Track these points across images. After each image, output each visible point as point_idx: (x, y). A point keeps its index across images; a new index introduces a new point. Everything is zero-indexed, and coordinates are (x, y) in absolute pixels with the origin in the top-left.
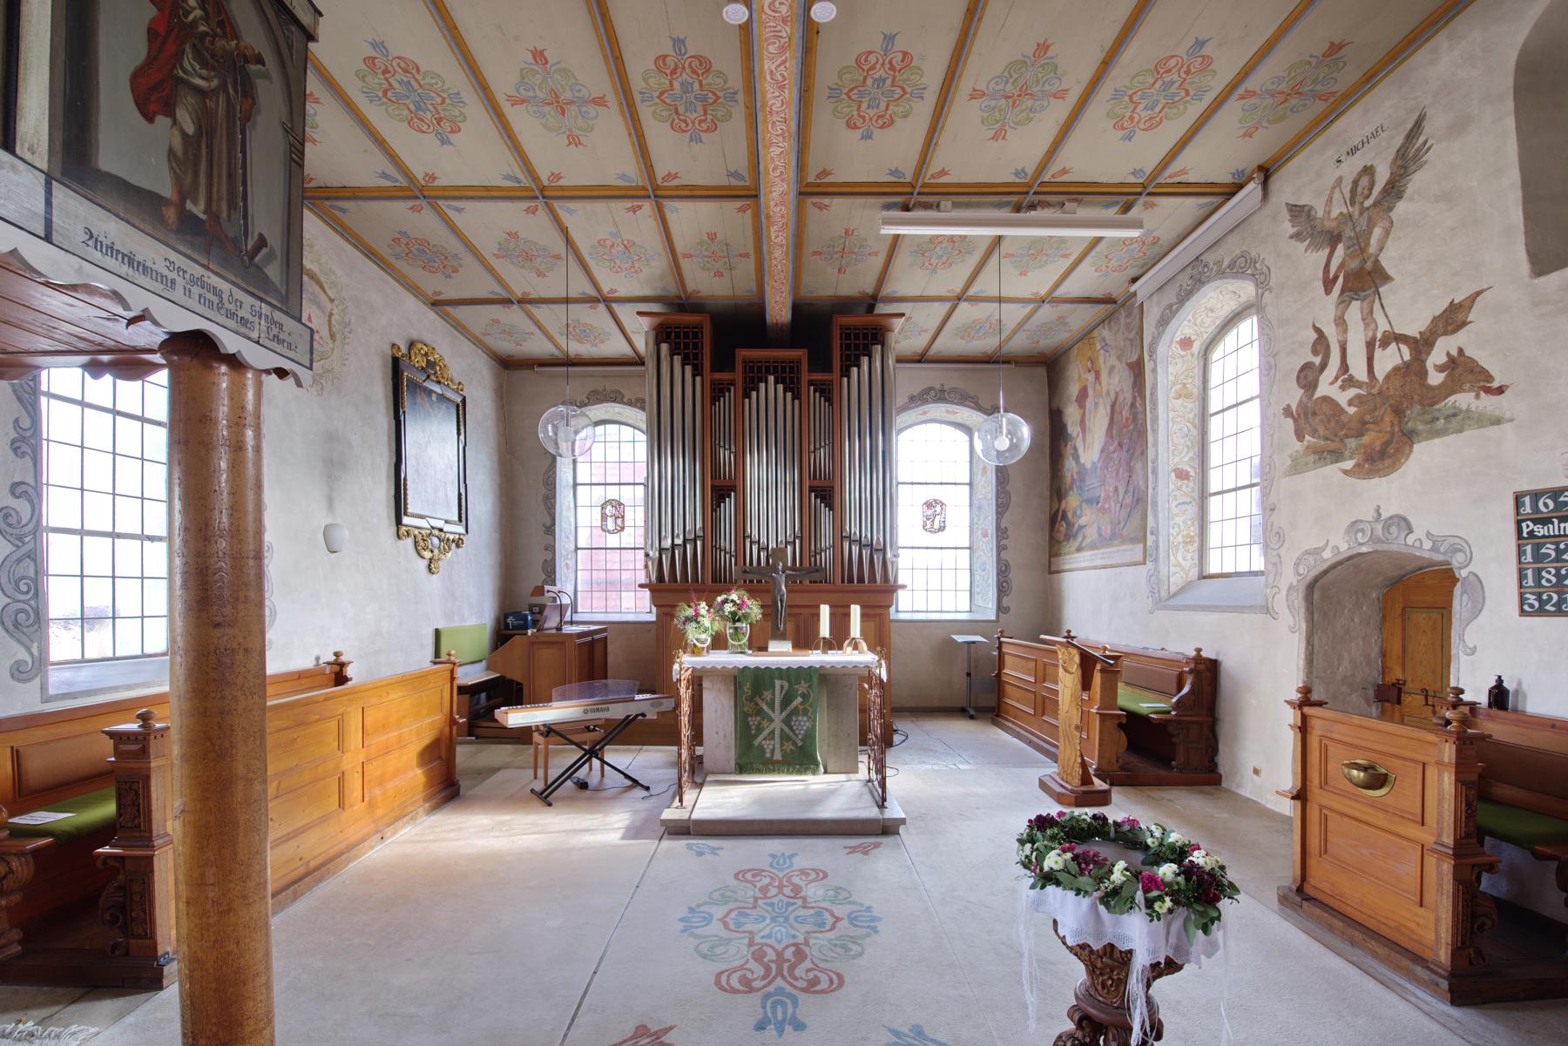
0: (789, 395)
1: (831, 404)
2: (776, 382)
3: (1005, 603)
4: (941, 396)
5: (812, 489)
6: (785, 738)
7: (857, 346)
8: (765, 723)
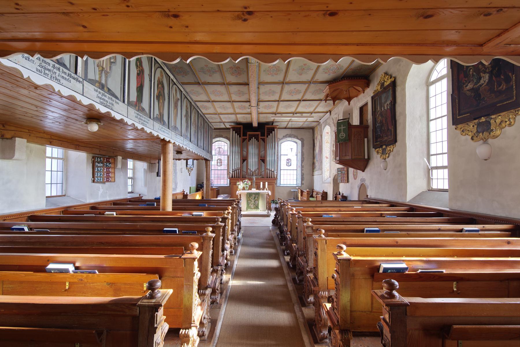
3: (303, 182)
4: (290, 136)
6: (254, 204)
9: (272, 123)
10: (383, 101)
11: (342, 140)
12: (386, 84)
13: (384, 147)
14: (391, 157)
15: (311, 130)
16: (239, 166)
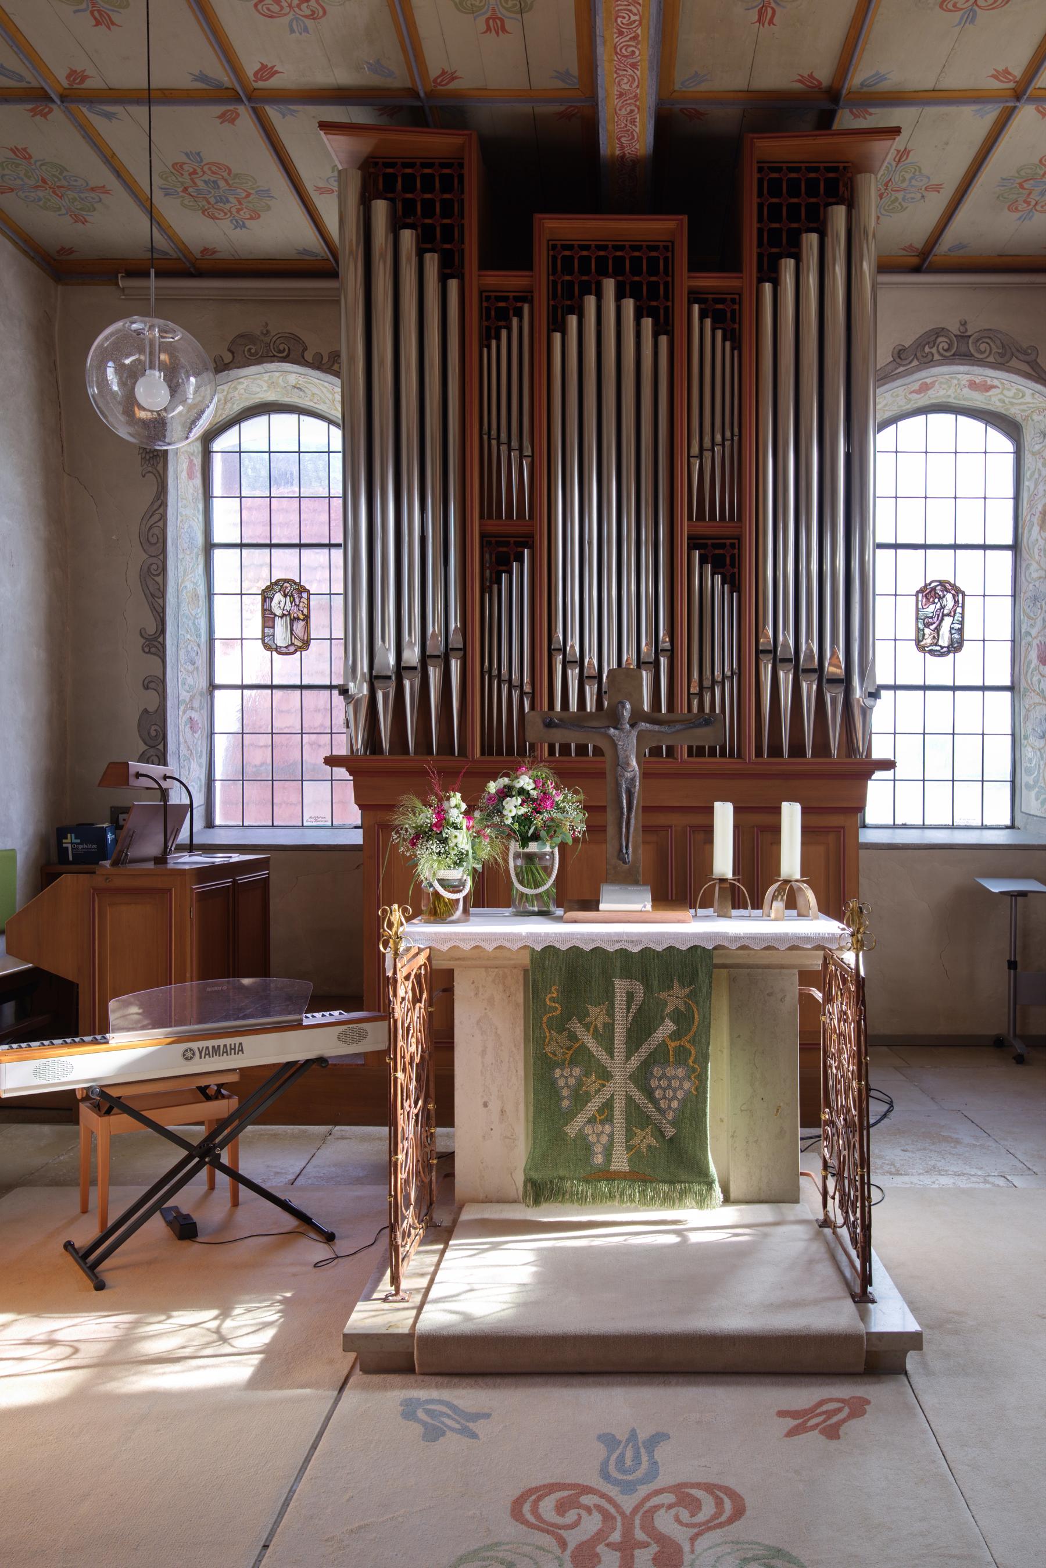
0: (647, 323)
1: (737, 346)
2: (620, 296)
5: (694, 543)
6: (636, 1118)
7: (794, 212)
8: (592, 1083)
16: (444, 618)
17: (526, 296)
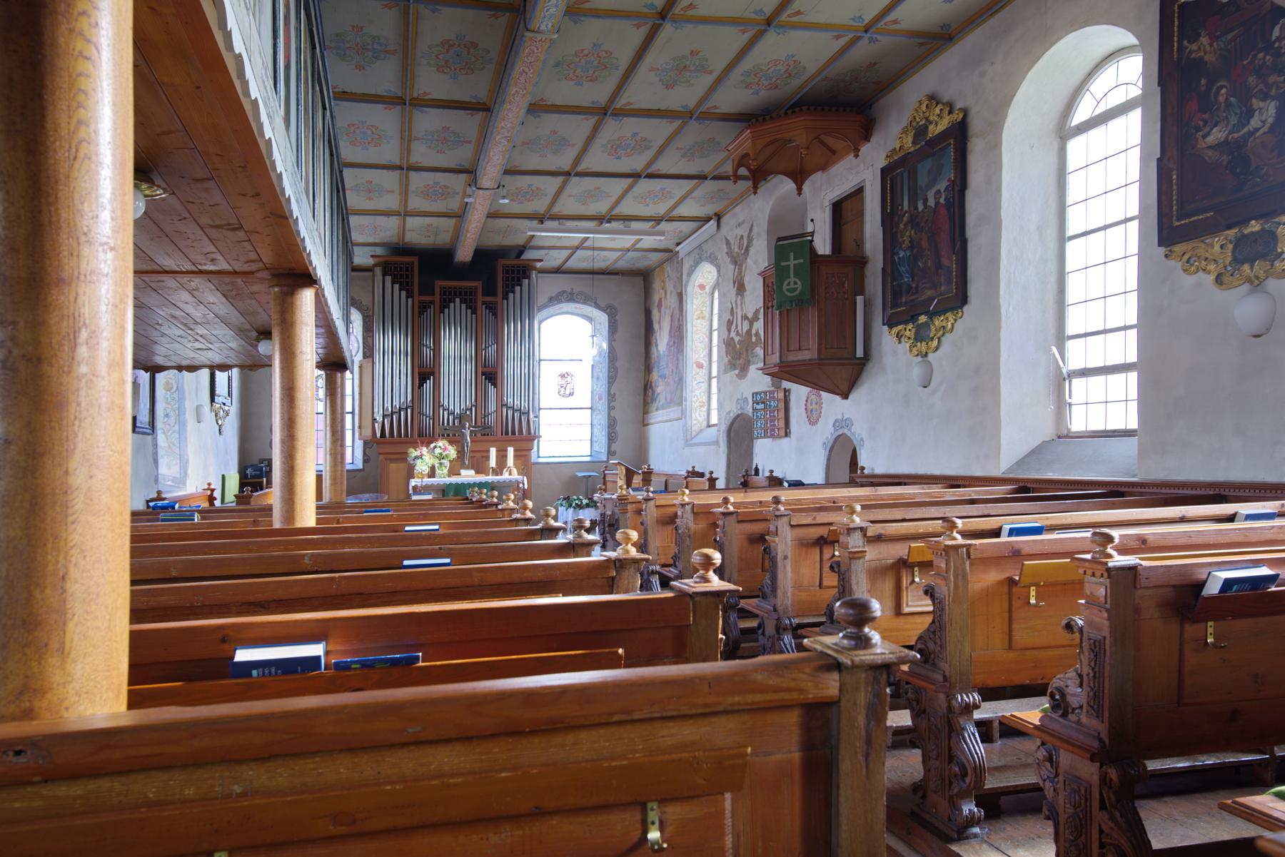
3: (613, 447)
4: (570, 297)
5: (483, 374)
9: (521, 250)
10: (922, 179)
11: (791, 301)
12: (934, 130)
13: (923, 319)
14: (946, 348)
15: (640, 280)
17: (433, 302)
